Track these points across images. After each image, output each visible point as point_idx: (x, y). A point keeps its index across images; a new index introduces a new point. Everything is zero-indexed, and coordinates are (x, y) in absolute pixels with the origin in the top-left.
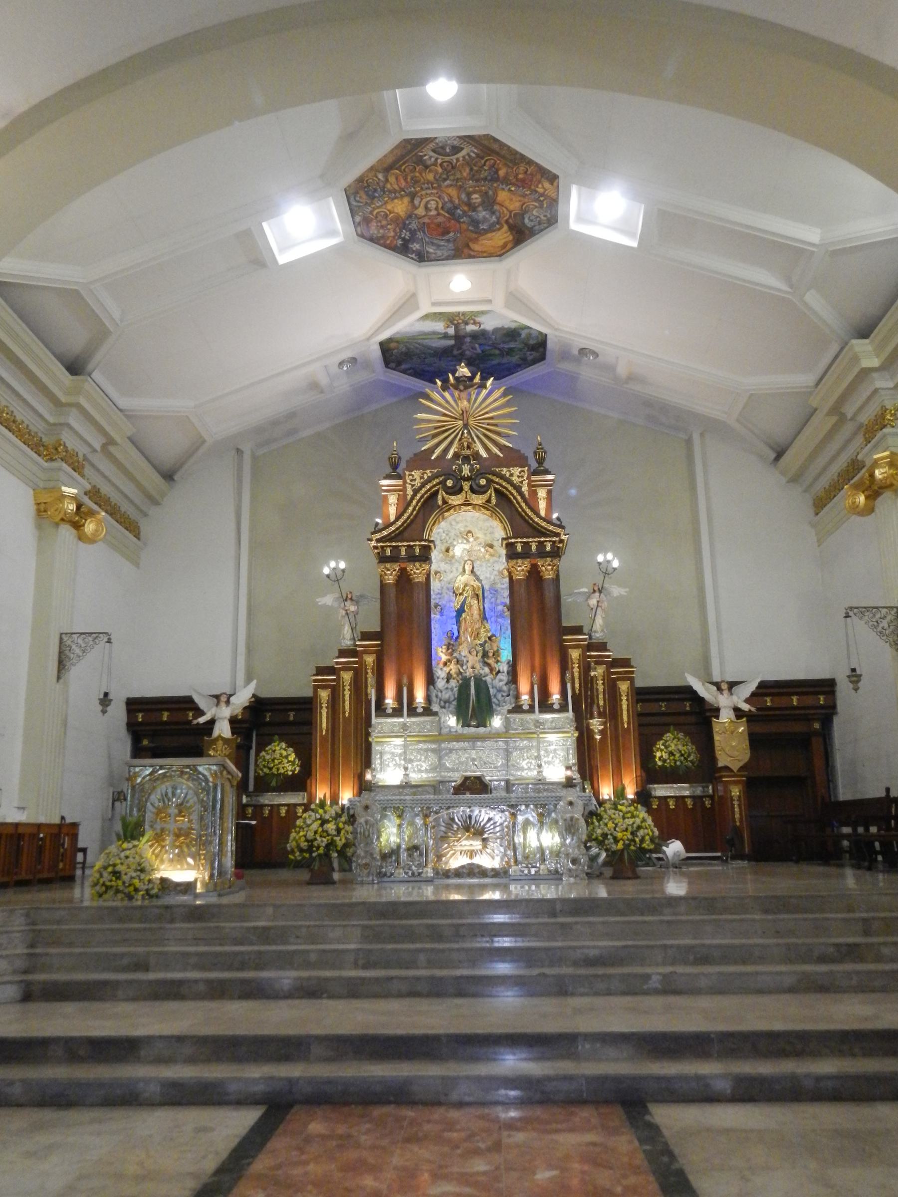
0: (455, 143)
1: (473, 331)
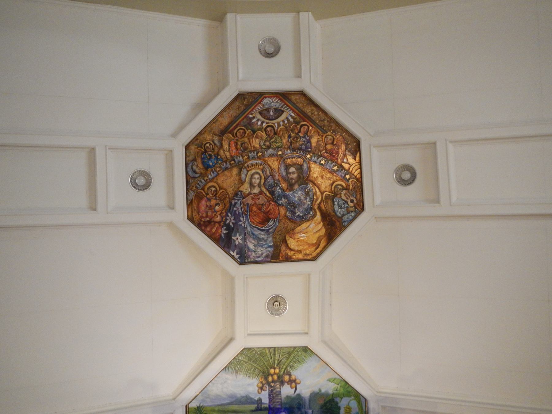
0: (278, 105)
1: (287, 397)
